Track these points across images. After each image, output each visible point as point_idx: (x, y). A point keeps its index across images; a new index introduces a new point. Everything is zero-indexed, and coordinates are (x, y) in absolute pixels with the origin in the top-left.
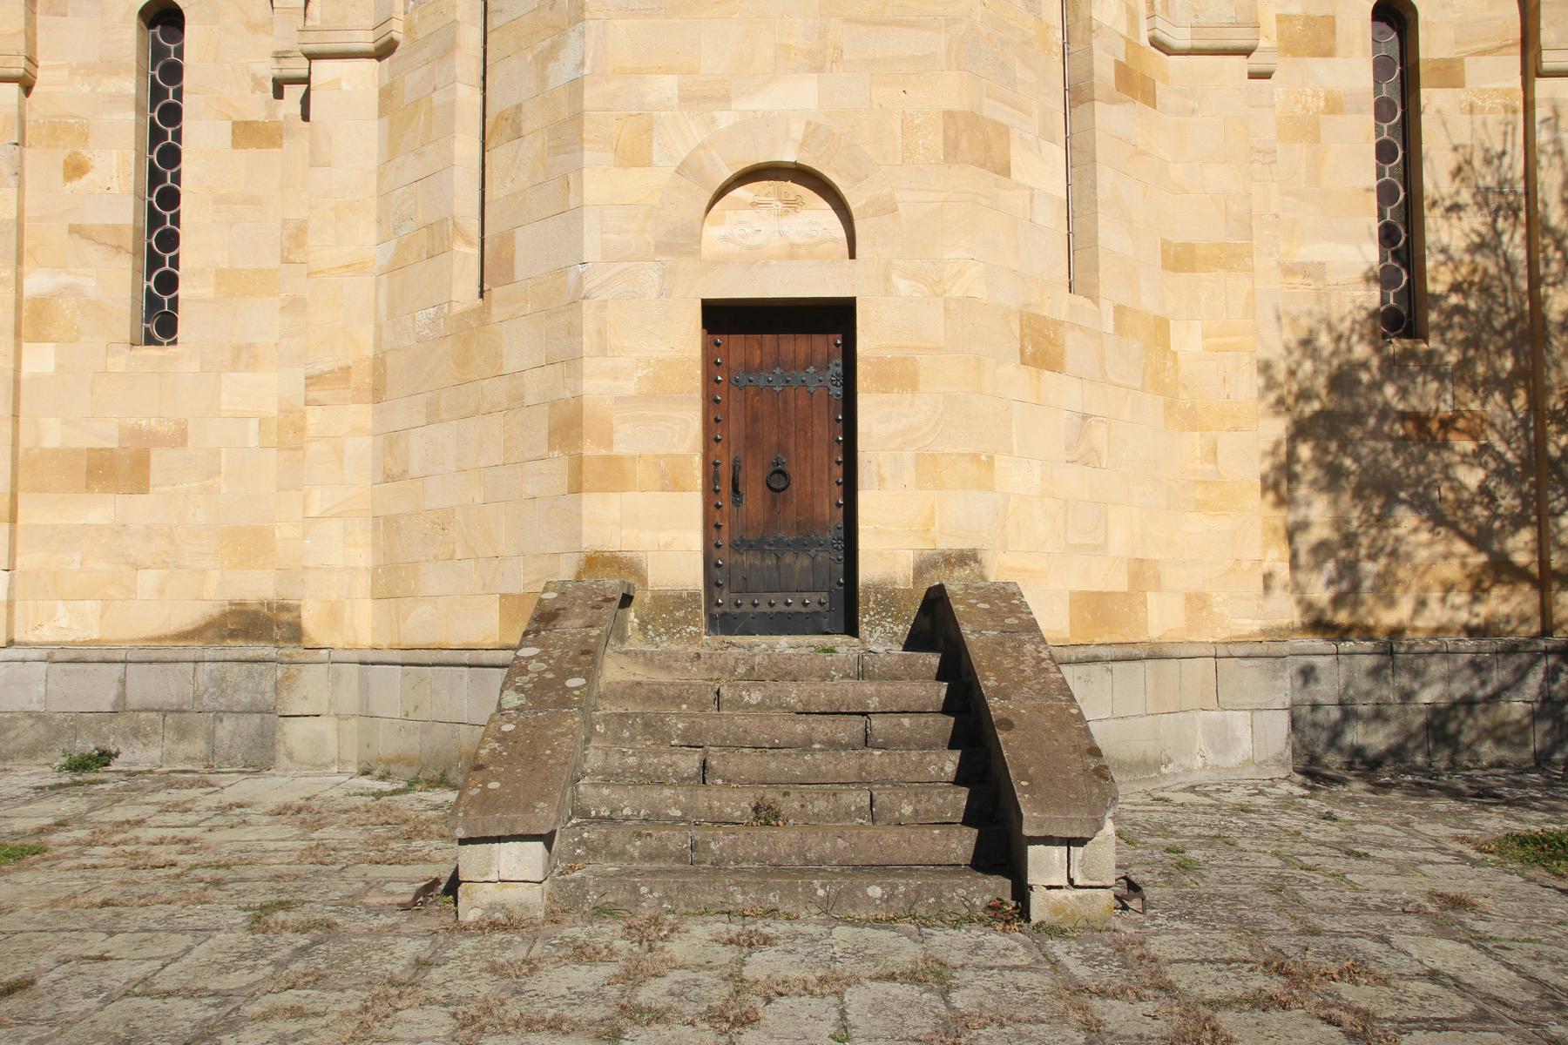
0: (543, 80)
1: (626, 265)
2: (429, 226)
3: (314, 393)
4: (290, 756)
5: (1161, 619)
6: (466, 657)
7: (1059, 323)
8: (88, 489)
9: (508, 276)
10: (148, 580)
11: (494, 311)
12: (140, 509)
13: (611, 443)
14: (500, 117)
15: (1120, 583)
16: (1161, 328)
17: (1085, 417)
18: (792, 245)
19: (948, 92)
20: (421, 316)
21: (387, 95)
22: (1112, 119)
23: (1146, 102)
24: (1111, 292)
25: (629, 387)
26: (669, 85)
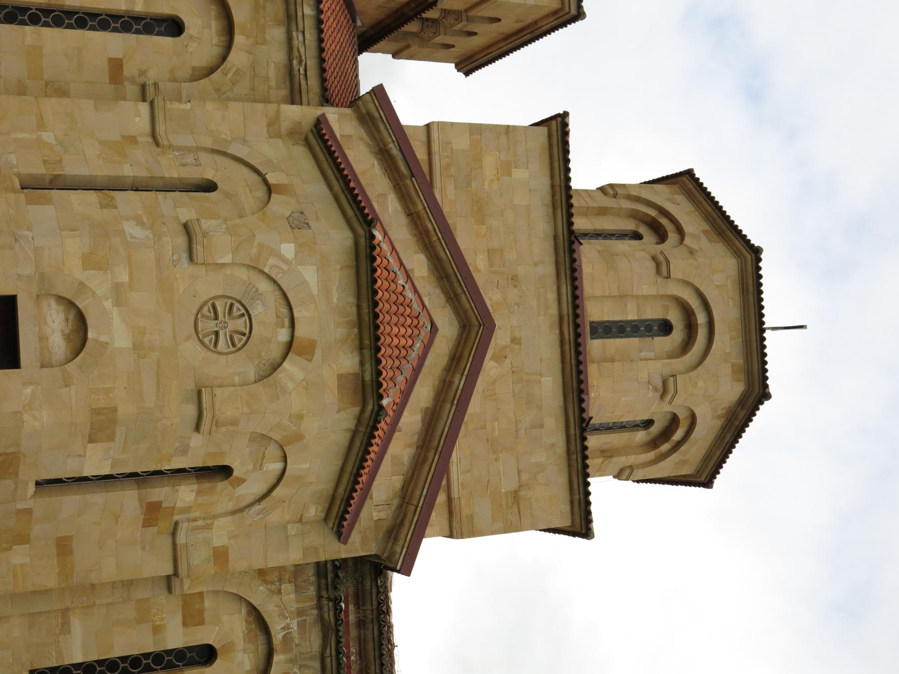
0: (127, 219)
1: (33, 258)
2: (60, 161)
7: (17, 475)
9: (30, 202)
11: (12, 195)
14: (113, 198)
16: (23, 539)
18: (47, 338)
19: (126, 410)
20: (13, 158)
21: (132, 140)
22: (129, 499)
23: (145, 520)
26: (124, 278)
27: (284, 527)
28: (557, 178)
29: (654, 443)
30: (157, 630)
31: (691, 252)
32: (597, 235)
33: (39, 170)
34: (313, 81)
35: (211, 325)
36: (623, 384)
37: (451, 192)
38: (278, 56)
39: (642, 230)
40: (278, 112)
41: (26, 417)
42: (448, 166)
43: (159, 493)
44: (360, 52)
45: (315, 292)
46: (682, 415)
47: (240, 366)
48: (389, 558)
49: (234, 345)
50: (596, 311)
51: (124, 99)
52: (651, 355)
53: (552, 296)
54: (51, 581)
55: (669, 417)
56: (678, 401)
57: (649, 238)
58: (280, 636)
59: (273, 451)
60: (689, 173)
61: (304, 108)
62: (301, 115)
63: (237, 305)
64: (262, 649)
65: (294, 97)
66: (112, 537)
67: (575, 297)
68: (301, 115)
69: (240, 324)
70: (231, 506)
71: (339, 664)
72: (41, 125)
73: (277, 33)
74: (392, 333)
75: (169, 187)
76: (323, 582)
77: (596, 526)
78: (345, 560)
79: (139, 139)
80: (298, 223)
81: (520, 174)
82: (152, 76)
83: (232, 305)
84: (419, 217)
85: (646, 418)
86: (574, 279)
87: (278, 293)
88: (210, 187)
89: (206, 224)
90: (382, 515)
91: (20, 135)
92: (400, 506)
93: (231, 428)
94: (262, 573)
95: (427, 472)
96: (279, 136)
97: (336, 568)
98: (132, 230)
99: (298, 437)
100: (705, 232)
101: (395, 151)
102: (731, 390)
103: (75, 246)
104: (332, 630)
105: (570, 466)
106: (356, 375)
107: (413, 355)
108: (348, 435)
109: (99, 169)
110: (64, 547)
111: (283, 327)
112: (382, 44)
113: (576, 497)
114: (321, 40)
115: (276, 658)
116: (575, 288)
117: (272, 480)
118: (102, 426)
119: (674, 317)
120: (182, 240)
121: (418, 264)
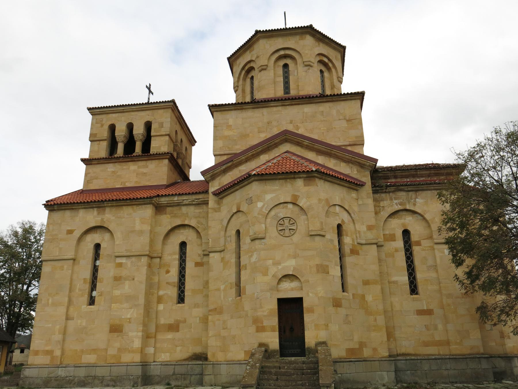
0: (250, 261)
2: (231, 283)
3: (210, 313)
4: (206, 383)
5: (367, 353)
6: (238, 362)
7: (341, 299)
8: (168, 331)
9: (245, 294)
10: (179, 349)
12: (178, 335)
13: (263, 324)
14: (243, 266)
15: (357, 346)
16: (363, 297)
17: (347, 315)
19: (317, 261)
20: (230, 299)
21: (223, 259)
22: (349, 260)
24: (351, 290)
25: (265, 314)
26: (271, 262)
27: (359, 205)
28: (232, 108)
29: (329, 69)
30: (397, 250)
31: (258, 57)
32: (252, 93)
33: (234, 290)
34: (200, 196)
35: (287, 231)
36: (307, 81)
37: (238, 147)
38: (192, 209)
39: (250, 76)
40: (211, 209)
41: (320, 295)
42: (229, 148)
43: (347, 249)
44: (189, 180)
45: (274, 195)
46: (318, 59)
47: (302, 221)
48: (371, 167)
49: (294, 223)
50: (280, 93)
51: (209, 262)
52: (296, 71)
53: (275, 109)
54: (379, 287)
55: (319, 64)
56: (313, 60)
57: (252, 73)
58: (400, 206)
59: (332, 209)
60: (229, 59)
61: (210, 199)
62: (212, 200)
63: (280, 222)
64: (404, 213)
65: (206, 203)
66: (363, 266)
67: (275, 100)
68: (212, 200)
69: (286, 221)
70: (352, 224)
71: (410, 185)
72: (218, 290)
73: (184, 209)
74: (289, 167)
75: (239, 247)
76: (380, 191)
77: (360, 90)
78: (372, 183)
79: (222, 256)
80: (250, 201)
81: (231, 122)
82: (200, 252)
83: (280, 224)
84: (247, 158)
85: (319, 73)
86: (268, 101)
87: (275, 208)
88: (238, 232)
89: (251, 233)
90: (355, 170)
91: (222, 297)
92: (352, 163)
93: (324, 224)
94: (376, 213)
95: (340, 154)
96: (220, 208)
97: (375, 186)
98: (253, 259)
99: (327, 200)
100: (250, 52)
101: (224, 167)
102: (309, 40)
103: (260, 279)
104: (398, 188)
105: (337, 101)
106: (304, 180)
107: (297, 159)
108: (326, 182)
109: (233, 270)
110: (366, 283)
111: (287, 206)
112: (186, 172)
113: (349, 98)
114: (186, 194)
115: (408, 208)
116: (272, 101)
117: (342, 209)
118: (323, 269)
119: (282, 63)
120: (257, 242)
121: (264, 158)
